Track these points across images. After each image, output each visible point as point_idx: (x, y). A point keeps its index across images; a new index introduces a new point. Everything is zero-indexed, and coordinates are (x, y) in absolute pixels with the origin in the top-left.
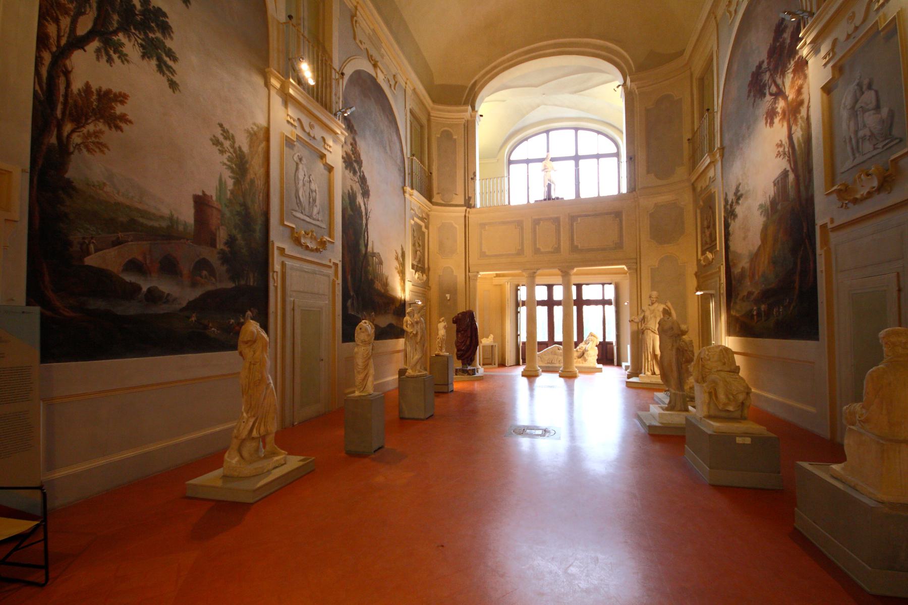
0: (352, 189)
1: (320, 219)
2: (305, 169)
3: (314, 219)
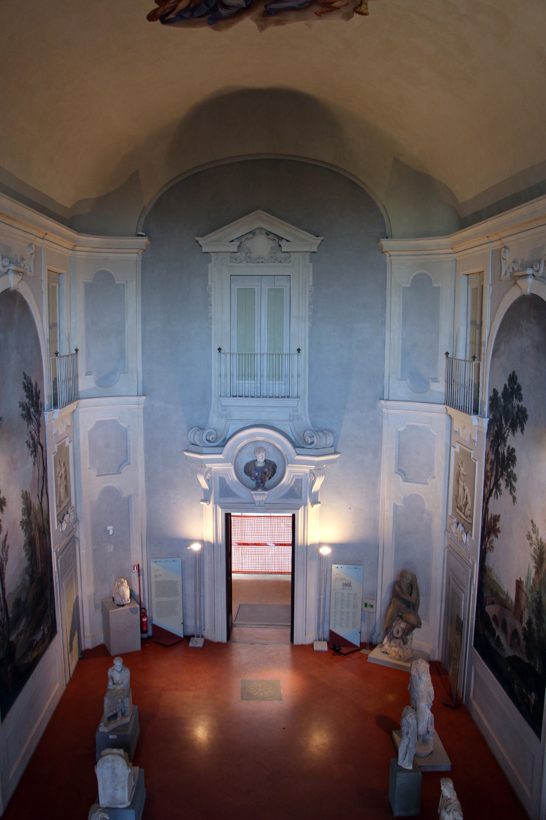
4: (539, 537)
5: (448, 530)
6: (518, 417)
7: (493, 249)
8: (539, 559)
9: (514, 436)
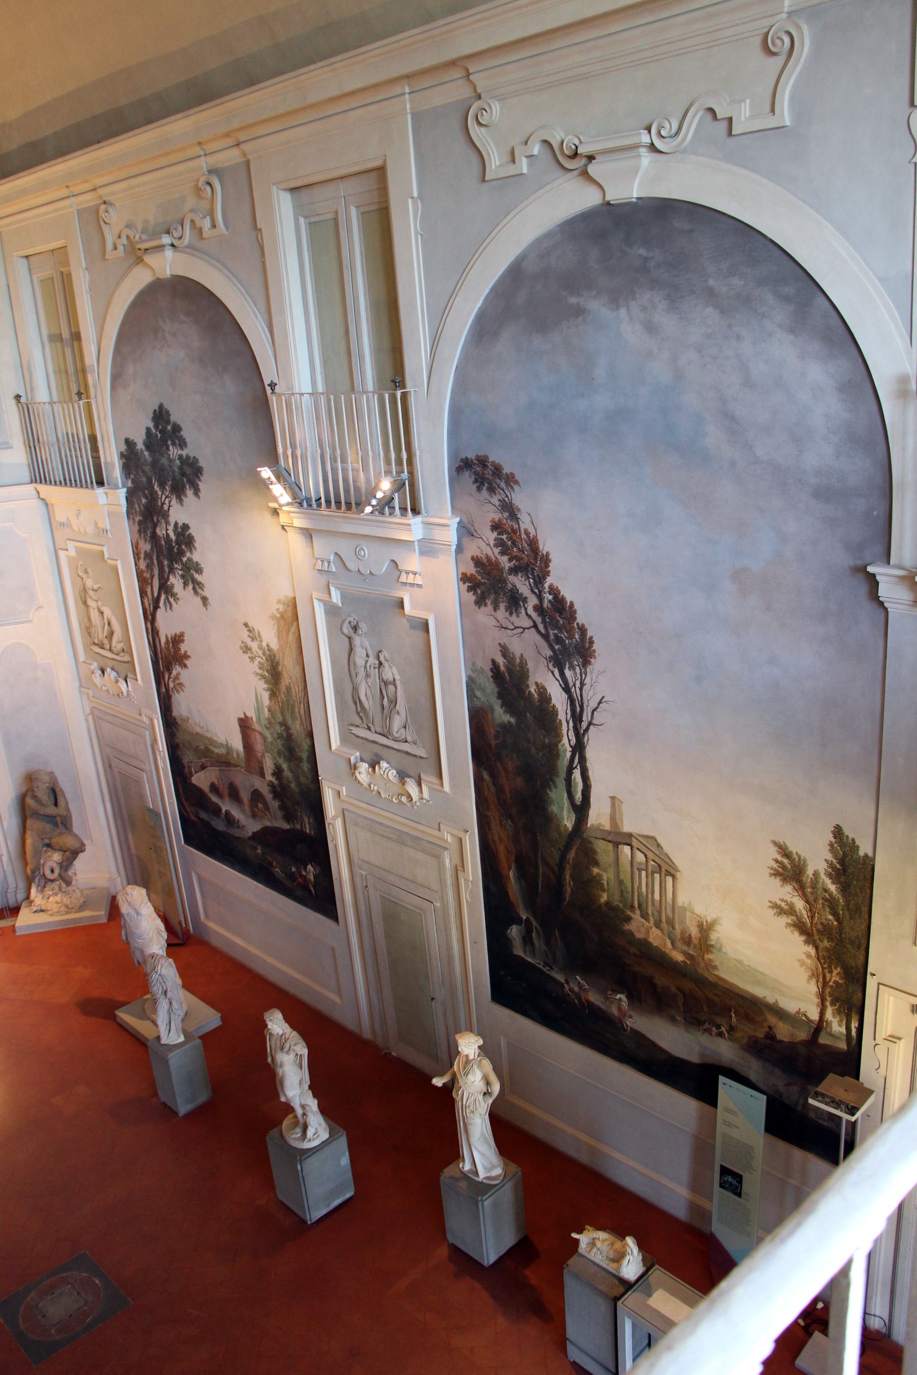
0: (505, 651)
1: (409, 739)
2: (367, 643)
3: (396, 740)
4: (264, 644)
5: (85, 683)
6: (183, 474)
7: (78, 208)
8: (272, 676)
9: (182, 505)
